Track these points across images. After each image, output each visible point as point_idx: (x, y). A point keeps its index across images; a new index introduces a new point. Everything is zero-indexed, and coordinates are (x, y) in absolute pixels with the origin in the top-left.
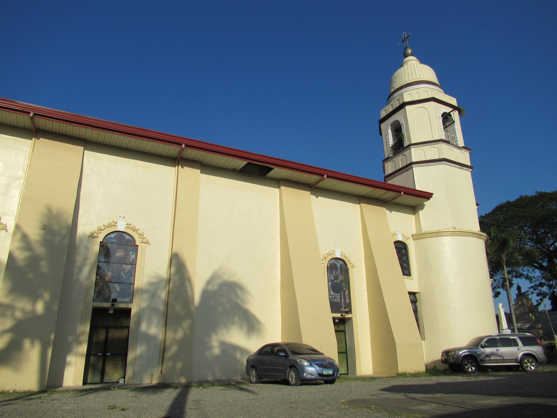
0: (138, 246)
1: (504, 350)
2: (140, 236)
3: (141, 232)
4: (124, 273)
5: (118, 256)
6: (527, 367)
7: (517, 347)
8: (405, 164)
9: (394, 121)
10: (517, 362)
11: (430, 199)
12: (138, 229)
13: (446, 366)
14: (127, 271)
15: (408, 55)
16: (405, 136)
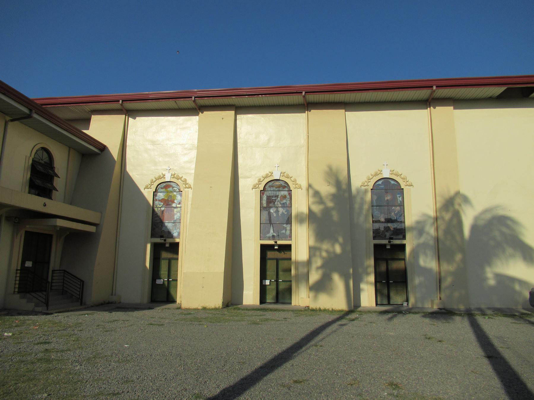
0: (403, 189)
2: (404, 180)
3: (404, 176)
5: (387, 200)
12: (400, 174)
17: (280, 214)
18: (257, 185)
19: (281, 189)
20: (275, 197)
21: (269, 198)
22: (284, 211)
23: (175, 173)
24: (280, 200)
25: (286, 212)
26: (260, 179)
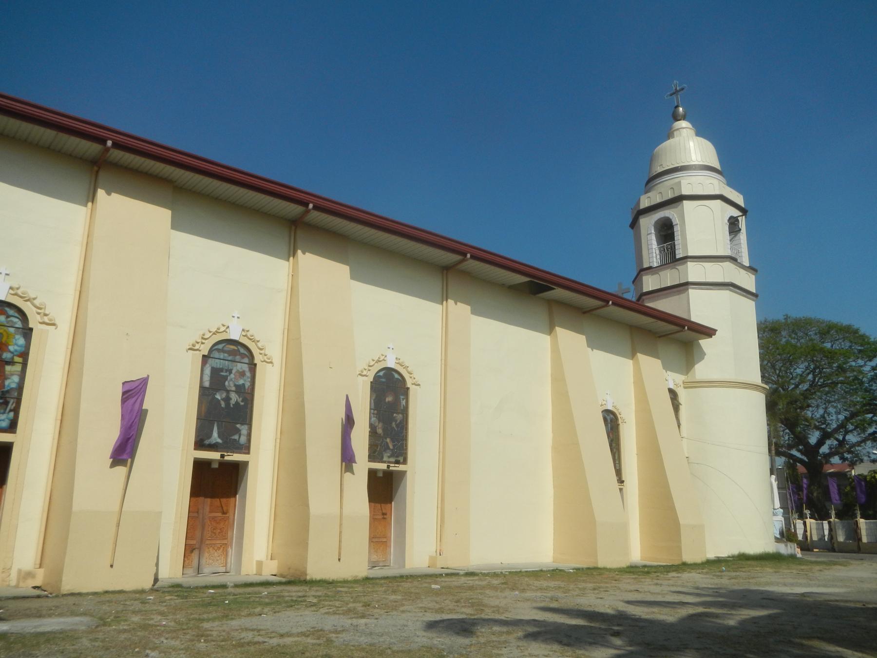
4: (395, 424)
5: (388, 402)
9: (662, 216)
11: (713, 336)
14: (398, 421)
17: (233, 405)
18: (197, 345)
19: (238, 358)
20: (227, 371)
21: (215, 372)
22: (240, 400)
25: (242, 401)
26: (204, 335)
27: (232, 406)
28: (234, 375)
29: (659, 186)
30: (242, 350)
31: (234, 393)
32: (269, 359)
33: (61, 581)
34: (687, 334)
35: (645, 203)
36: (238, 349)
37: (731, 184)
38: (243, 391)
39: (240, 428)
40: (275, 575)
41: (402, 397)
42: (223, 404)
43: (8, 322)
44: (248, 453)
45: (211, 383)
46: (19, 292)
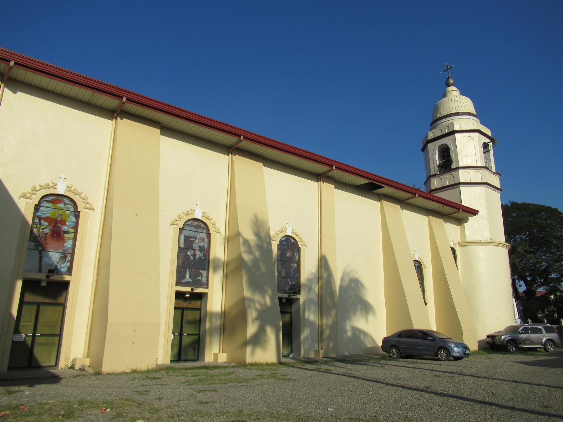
0: (79, 212)
1: (534, 336)
2: (84, 201)
3: (214, 222)
5: (288, 256)
6: (548, 349)
7: (542, 334)
8: (453, 183)
9: (442, 144)
10: (542, 345)
12: (80, 192)
13: (488, 346)
14: (294, 268)
15: (451, 85)
16: (453, 159)
17: (198, 258)
18: (176, 221)
19: (200, 230)
20: (194, 238)
21: (187, 238)
23: (71, 185)
24: (198, 242)
27: (197, 259)
28: (198, 240)
29: (439, 125)
30: (202, 225)
31: (198, 251)
32: (218, 231)
33: (102, 366)
34: (461, 214)
35: (431, 136)
36: (200, 224)
37: (482, 123)
38: (203, 250)
39: (202, 273)
40: (225, 362)
41: (296, 253)
42: (192, 258)
43: (66, 208)
44: (207, 288)
45: (184, 245)
46: (72, 189)
